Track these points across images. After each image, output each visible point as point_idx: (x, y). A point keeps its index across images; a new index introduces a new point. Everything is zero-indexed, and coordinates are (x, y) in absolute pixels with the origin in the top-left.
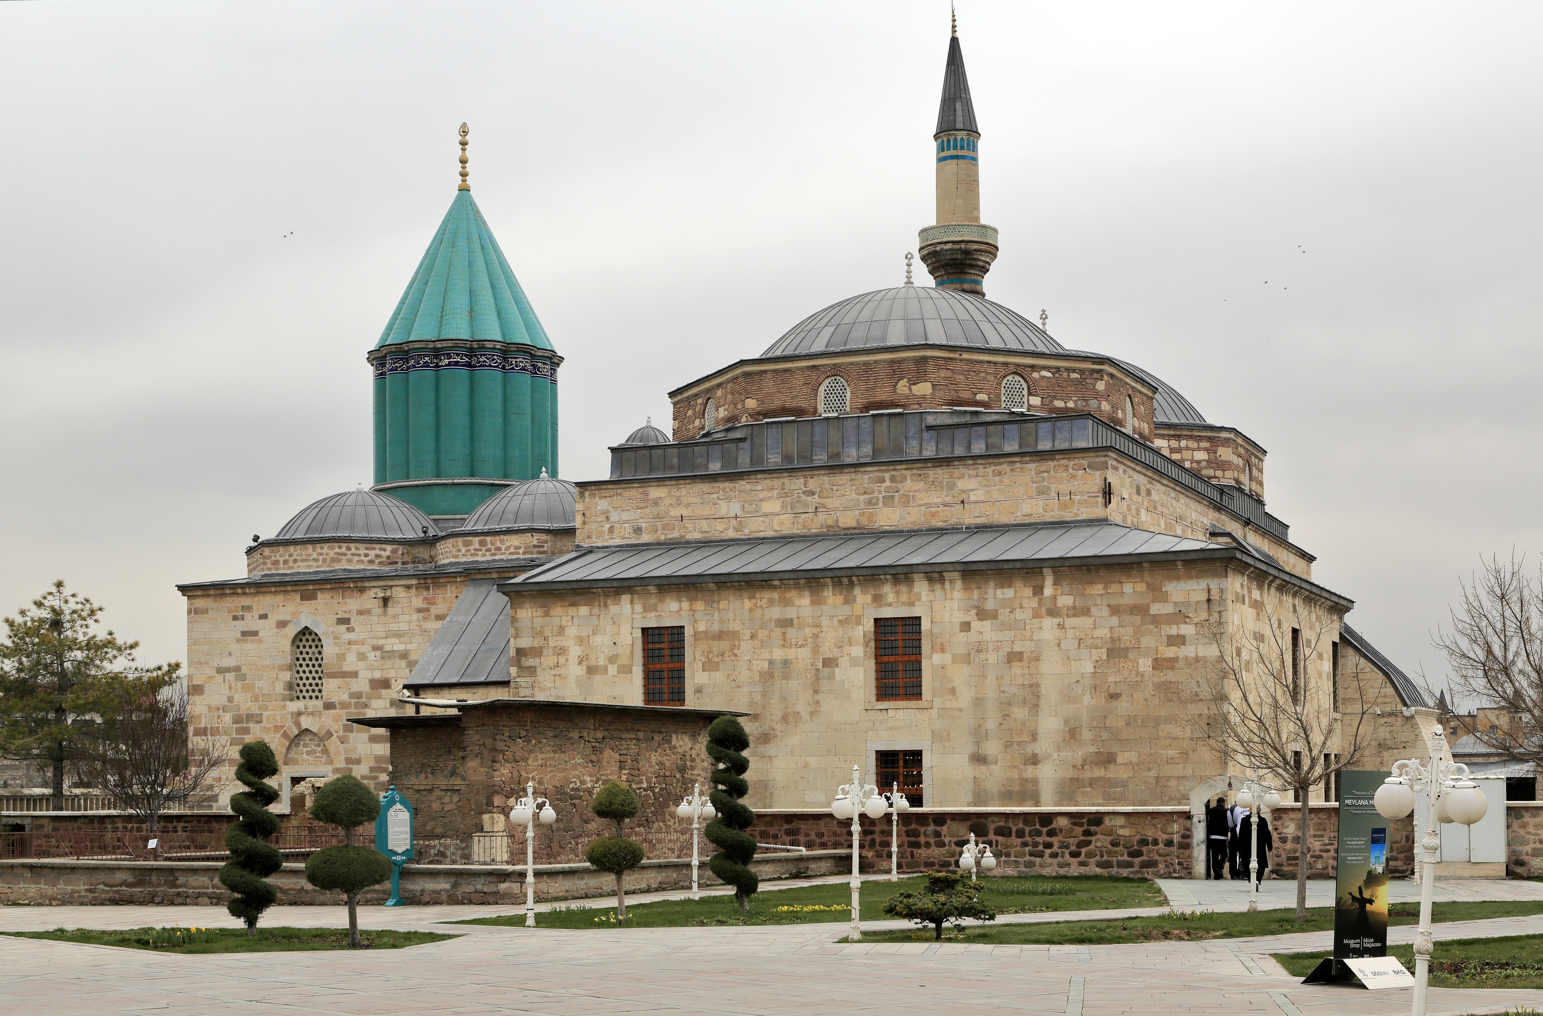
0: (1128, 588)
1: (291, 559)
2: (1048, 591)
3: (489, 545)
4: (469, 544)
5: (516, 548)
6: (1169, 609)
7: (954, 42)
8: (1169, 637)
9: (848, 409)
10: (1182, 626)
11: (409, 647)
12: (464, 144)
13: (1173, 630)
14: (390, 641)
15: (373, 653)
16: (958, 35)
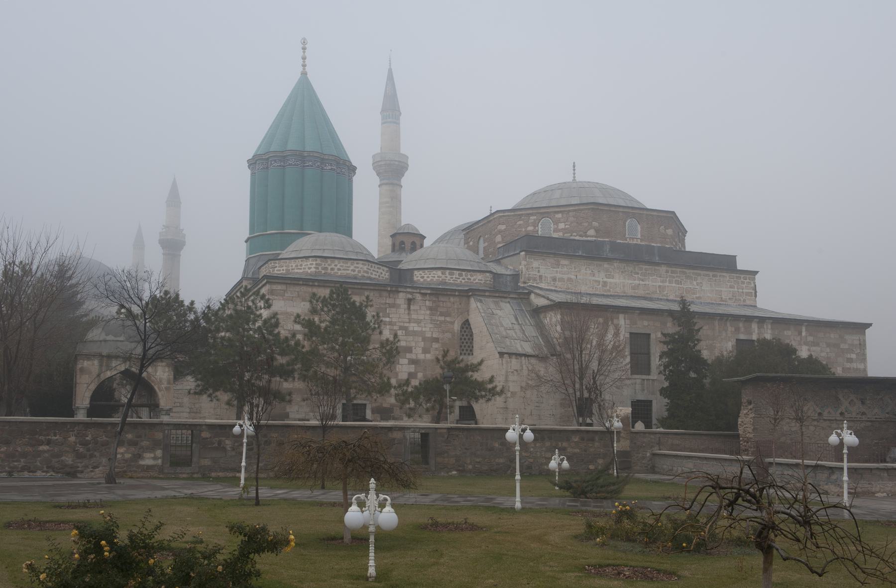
0: (832, 336)
1: (336, 268)
2: (804, 334)
3: (464, 277)
4: (453, 274)
5: (479, 280)
6: (846, 346)
7: (390, 70)
8: (847, 358)
9: (639, 236)
10: (851, 354)
11: (424, 329)
12: (304, 49)
13: (849, 356)
14: (412, 325)
15: (401, 331)
16: (392, 67)
